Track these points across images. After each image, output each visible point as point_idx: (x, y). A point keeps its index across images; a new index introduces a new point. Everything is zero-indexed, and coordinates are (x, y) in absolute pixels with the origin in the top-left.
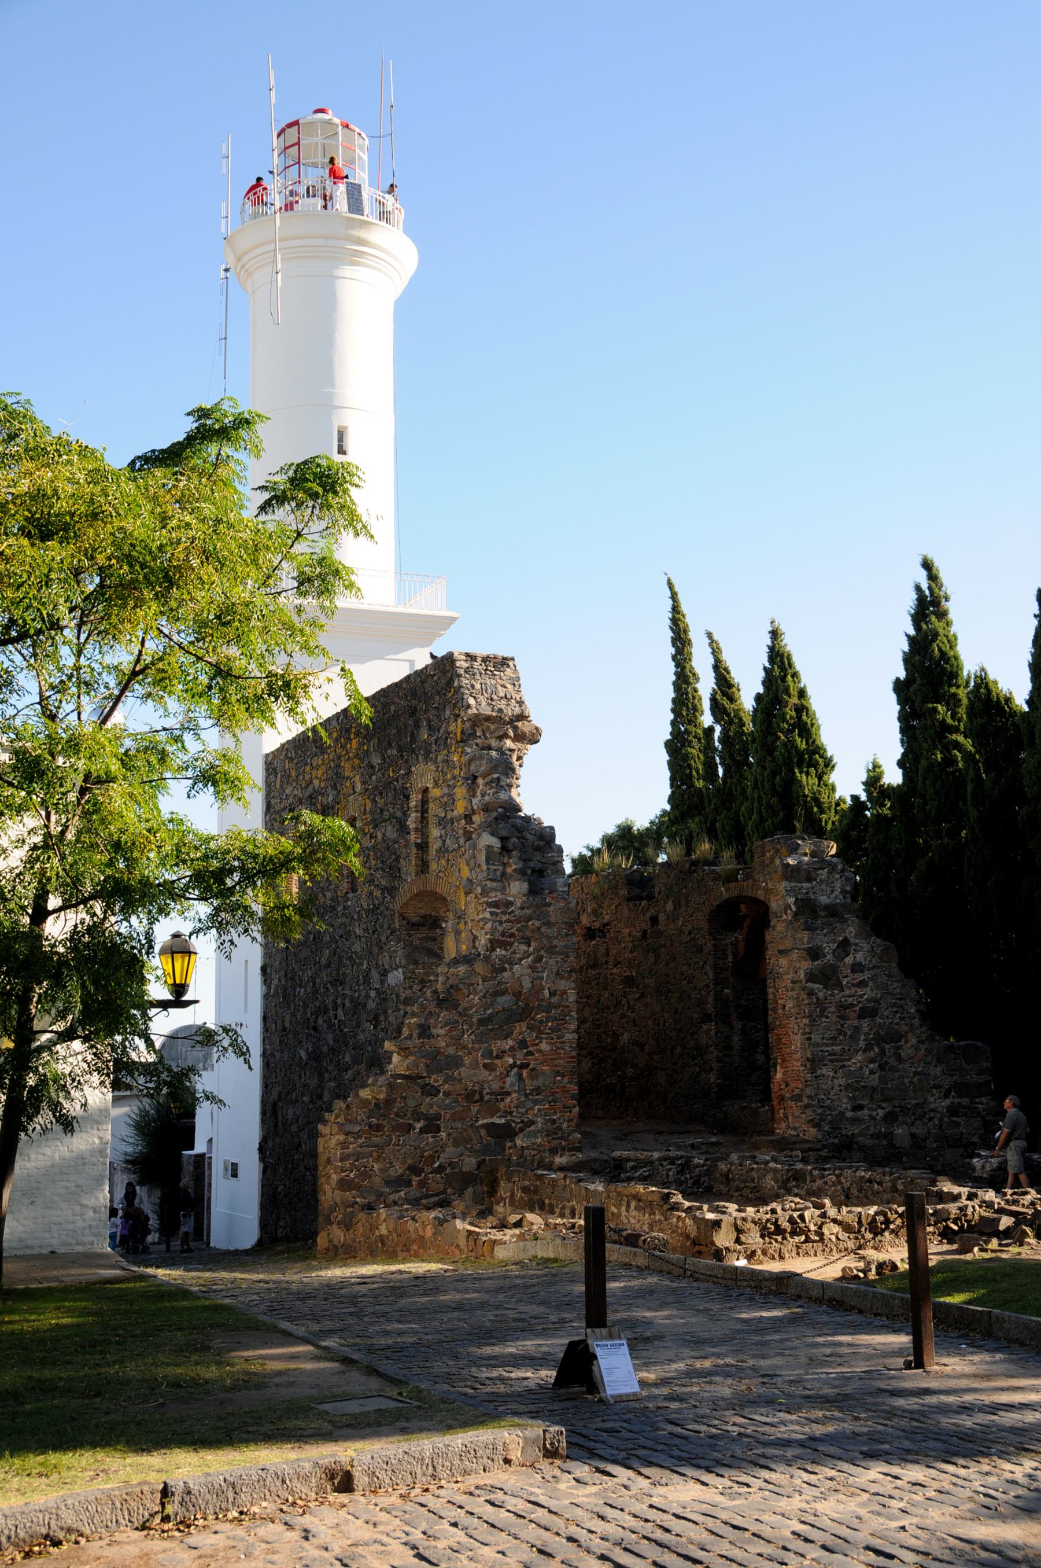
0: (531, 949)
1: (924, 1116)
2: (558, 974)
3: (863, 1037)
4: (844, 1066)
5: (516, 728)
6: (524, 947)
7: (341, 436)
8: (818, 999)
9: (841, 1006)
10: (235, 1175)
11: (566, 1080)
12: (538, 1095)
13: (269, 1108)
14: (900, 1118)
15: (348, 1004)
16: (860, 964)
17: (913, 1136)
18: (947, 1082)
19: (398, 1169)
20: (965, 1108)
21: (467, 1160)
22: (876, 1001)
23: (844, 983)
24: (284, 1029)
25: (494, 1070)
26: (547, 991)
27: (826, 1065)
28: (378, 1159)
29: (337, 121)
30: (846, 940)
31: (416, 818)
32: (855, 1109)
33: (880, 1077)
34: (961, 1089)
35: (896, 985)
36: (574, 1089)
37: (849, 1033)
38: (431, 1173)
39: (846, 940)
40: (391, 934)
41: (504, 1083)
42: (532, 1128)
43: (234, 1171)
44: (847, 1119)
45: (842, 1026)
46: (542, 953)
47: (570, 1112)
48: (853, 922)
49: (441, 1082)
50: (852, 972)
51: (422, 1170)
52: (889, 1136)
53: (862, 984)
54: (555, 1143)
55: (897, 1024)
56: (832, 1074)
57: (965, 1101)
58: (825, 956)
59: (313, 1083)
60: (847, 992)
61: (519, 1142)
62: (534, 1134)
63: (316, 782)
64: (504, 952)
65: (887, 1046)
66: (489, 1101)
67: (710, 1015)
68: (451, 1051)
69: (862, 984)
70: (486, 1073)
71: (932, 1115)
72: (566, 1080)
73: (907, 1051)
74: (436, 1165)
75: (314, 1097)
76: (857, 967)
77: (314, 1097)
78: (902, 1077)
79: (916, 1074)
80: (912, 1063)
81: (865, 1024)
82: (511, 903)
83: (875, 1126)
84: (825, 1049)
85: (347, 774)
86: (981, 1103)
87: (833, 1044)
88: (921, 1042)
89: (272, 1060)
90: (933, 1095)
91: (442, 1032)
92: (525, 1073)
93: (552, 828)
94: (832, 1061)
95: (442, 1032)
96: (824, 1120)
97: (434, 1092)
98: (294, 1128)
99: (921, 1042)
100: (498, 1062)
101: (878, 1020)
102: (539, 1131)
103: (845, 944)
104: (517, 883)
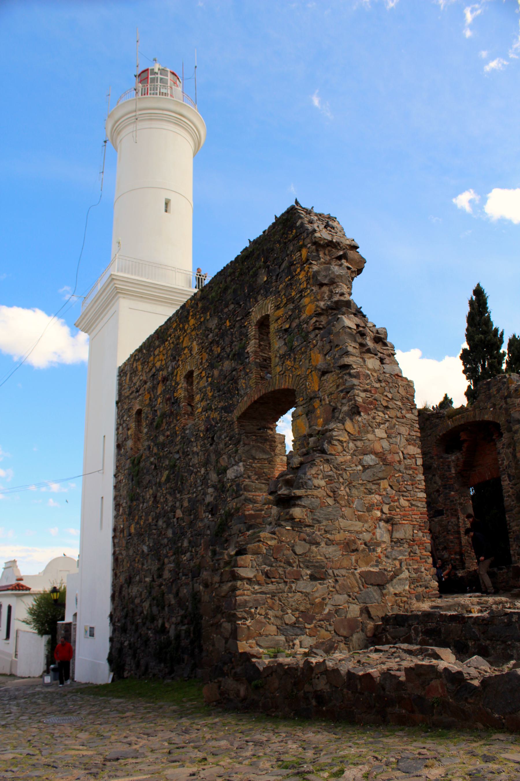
0: (387, 416)
5: (348, 257)
6: (381, 414)
10: (92, 635)
12: (401, 546)
13: (118, 589)
15: (186, 504)
19: (290, 618)
21: (352, 606)
24: (130, 534)
25: (366, 521)
26: (401, 454)
28: (271, 608)
29: (168, 70)
31: (255, 344)
36: (427, 540)
38: (320, 621)
40: (230, 440)
41: (374, 534)
42: (402, 576)
43: (92, 633)
49: (323, 532)
51: (313, 618)
59: (155, 567)
61: (391, 589)
63: (158, 364)
64: (366, 417)
66: (364, 550)
67: (442, 510)
70: (361, 524)
74: (326, 611)
75: (155, 577)
77: (155, 577)
82: (367, 376)
85: (185, 345)
89: (120, 557)
91: (322, 483)
93: (385, 329)
95: (322, 483)
97: (319, 540)
98: (137, 601)
104: (372, 360)
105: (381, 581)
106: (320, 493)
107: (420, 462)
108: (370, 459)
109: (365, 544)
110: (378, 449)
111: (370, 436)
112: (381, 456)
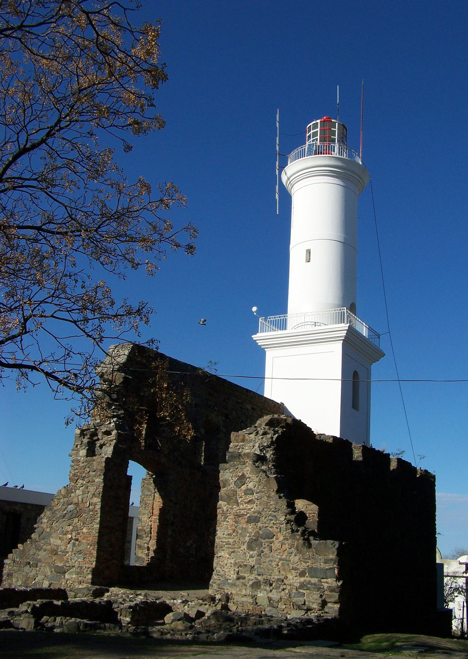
0: (84, 482)
1: (279, 587)
2: (94, 494)
3: (248, 535)
4: (234, 552)
6: (81, 481)
7: (309, 252)
8: (223, 511)
9: (236, 515)
11: (91, 548)
14: (262, 586)
16: (251, 489)
17: (270, 599)
18: (302, 566)
20: (312, 584)
22: (259, 513)
23: (239, 501)
25: (63, 540)
27: (224, 550)
30: (243, 475)
32: (238, 579)
33: (256, 560)
34: (313, 572)
35: (272, 502)
37: (240, 531)
39: (243, 475)
41: (67, 547)
44: (229, 583)
45: (236, 527)
46: (89, 484)
47: (92, 564)
48: (249, 464)
50: (245, 494)
52: (254, 597)
53: (250, 502)
54: (80, 579)
55: (271, 527)
56: (228, 556)
57: (314, 580)
58: (229, 485)
60: (241, 507)
61: (67, 576)
62: (72, 573)
65: (263, 541)
68: (48, 530)
69: (250, 502)
70: (60, 541)
71: (284, 587)
72: (91, 548)
73: (276, 545)
76: (249, 492)
78: (272, 561)
79: (280, 559)
80: (279, 552)
81: (250, 527)
83: (246, 589)
84: (224, 540)
86: (327, 582)
87: (229, 538)
88: (286, 539)
90: (292, 575)
92: (77, 542)
94: (228, 548)
96: (215, 583)
99: (286, 539)
100: (65, 536)
101: (260, 524)
102: (74, 572)
103: (242, 479)
105: (62, 571)
106: (45, 526)
107: (98, 506)
108: (71, 507)
109: (61, 551)
110: (75, 500)
111: (72, 495)
112: (77, 504)
